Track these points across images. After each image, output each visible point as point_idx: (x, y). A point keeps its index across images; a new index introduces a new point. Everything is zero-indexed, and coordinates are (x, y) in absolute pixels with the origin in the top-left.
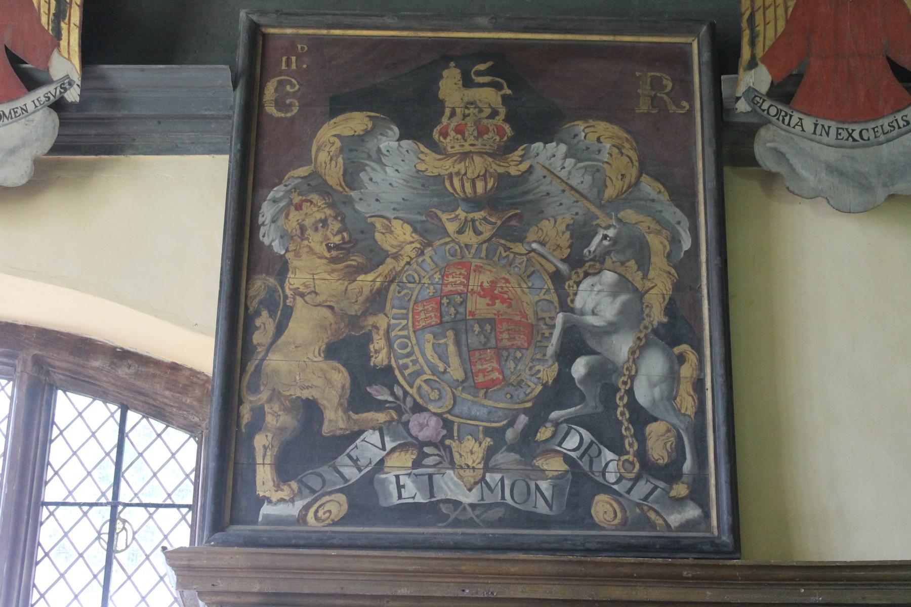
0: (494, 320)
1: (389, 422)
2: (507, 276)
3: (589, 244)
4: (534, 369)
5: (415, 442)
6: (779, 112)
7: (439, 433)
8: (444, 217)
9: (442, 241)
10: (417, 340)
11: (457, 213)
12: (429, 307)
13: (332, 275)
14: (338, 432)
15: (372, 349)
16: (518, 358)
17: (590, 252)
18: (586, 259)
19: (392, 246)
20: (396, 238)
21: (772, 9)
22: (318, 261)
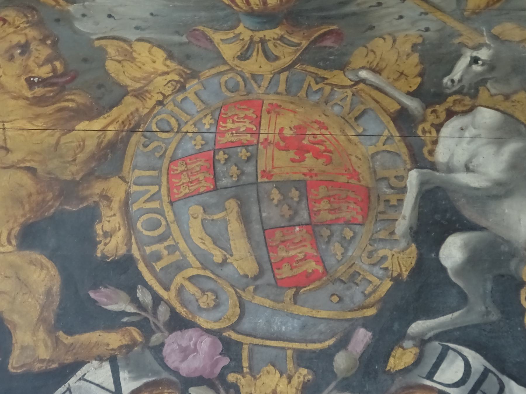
0: (305, 182)
1: (129, 347)
2: (322, 119)
3: (449, 71)
4: (375, 255)
5: (174, 378)
7: (217, 362)
8: (217, 37)
9: (214, 71)
10: (175, 214)
11: (237, 31)
12: (196, 166)
13: (35, 123)
14: (37, 367)
15: (100, 232)
16: (348, 238)
17: (453, 81)
18: (448, 91)
19: (134, 79)
20: (140, 68)
22: (13, 102)
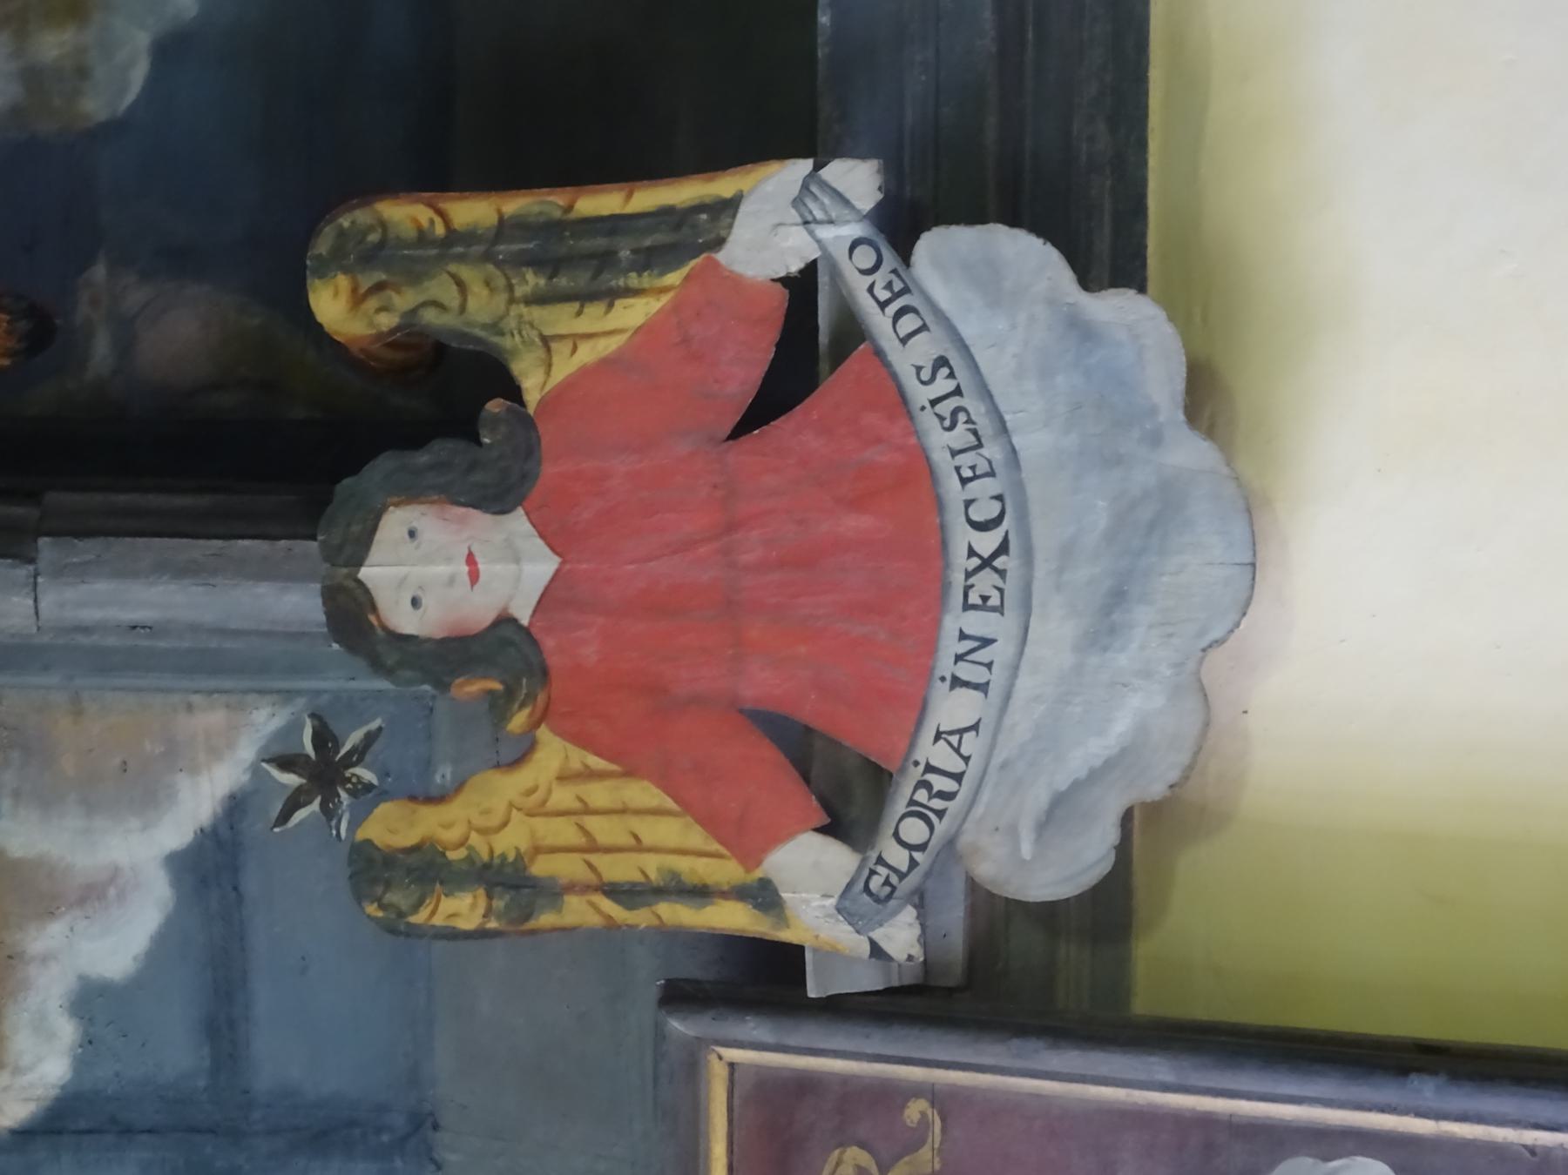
6: (916, 811)
21: (593, 823)
